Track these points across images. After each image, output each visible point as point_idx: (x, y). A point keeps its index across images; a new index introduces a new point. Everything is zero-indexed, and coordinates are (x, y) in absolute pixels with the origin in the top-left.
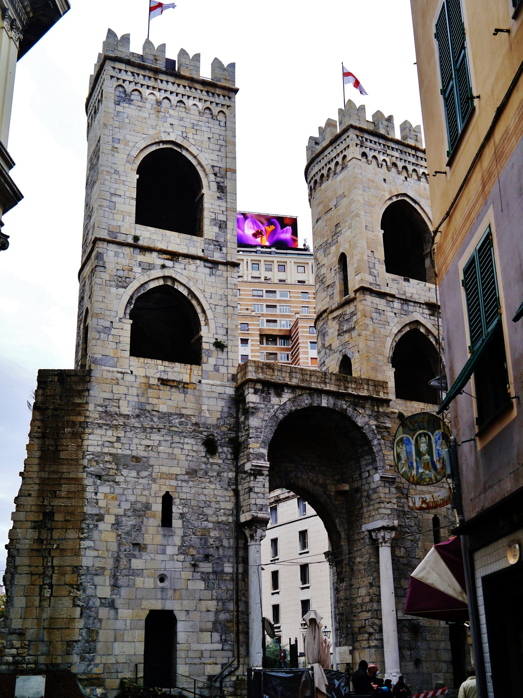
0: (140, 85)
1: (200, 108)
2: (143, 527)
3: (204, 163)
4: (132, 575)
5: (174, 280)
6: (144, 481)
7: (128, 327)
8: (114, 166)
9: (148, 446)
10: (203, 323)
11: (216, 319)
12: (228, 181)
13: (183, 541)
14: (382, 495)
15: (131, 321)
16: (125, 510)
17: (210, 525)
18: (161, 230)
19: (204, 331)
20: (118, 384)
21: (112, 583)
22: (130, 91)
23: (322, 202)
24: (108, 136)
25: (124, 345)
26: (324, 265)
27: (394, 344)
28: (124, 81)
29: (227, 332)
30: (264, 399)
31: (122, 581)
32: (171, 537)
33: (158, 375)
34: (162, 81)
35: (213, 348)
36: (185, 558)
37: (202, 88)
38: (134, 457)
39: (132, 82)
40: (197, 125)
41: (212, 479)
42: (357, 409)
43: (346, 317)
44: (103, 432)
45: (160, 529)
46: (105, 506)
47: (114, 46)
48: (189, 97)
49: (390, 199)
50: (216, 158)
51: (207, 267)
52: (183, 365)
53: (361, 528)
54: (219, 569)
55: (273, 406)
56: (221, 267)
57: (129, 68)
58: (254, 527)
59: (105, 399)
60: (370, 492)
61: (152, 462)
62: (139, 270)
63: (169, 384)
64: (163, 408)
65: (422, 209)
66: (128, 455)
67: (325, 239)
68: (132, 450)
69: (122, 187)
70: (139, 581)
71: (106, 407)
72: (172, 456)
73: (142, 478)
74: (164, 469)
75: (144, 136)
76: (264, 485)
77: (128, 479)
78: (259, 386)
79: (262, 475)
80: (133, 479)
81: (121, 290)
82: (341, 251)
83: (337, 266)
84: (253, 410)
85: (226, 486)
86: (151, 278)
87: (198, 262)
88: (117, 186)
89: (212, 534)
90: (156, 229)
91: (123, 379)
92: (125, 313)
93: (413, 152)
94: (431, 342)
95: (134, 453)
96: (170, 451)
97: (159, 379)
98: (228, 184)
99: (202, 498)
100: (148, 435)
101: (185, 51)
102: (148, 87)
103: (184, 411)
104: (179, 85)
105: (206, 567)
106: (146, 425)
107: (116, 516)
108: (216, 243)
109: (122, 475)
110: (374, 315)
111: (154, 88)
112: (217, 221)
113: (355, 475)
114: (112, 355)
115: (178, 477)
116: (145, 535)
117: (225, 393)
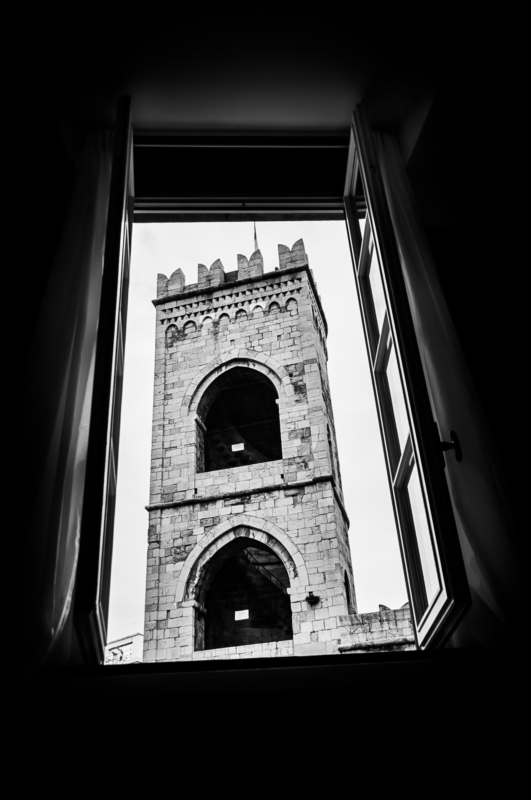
0: (193, 315)
1: (264, 307)
5: (249, 528)
8: (167, 416)
10: (291, 575)
11: (307, 563)
18: (226, 470)
22: (182, 326)
24: (159, 385)
25: (183, 638)
28: (176, 319)
29: (325, 578)
39: (184, 316)
40: (263, 328)
47: (163, 289)
48: (250, 302)
50: (290, 355)
51: (289, 496)
56: (307, 489)
57: (181, 303)
69: (178, 436)
75: (201, 368)
86: (216, 537)
87: (276, 493)
88: (172, 438)
90: (220, 471)
92: (187, 593)
101: (241, 255)
102: (202, 313)
104: (237, 295)
108: (298, 460)
111: (209, 311)
112: (298, 431)
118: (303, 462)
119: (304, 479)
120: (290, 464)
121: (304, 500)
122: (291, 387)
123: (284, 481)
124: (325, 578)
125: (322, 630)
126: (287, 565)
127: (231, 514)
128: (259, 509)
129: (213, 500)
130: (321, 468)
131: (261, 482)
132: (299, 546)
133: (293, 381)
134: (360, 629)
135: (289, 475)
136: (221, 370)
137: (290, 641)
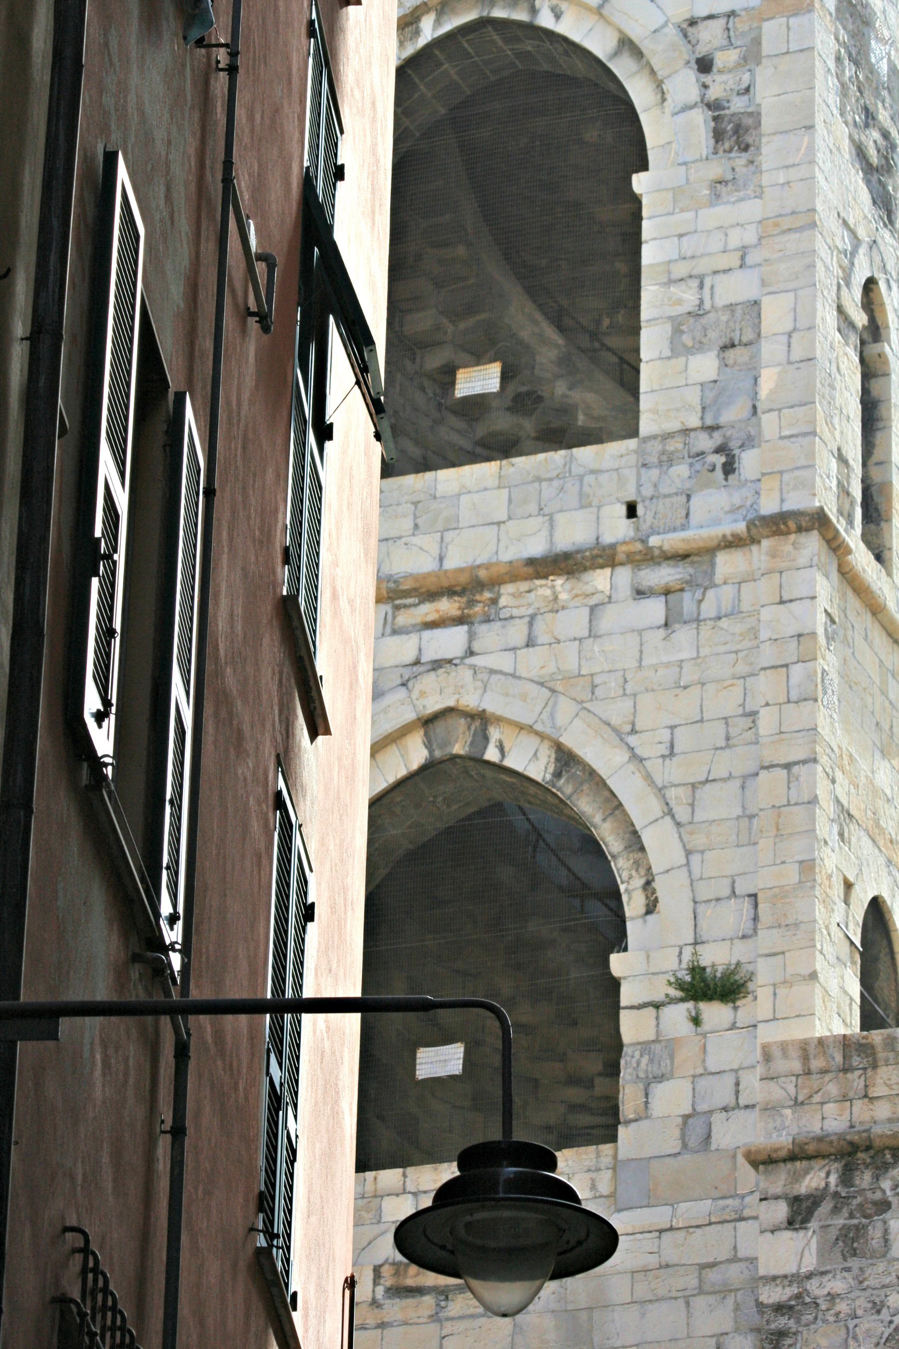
5: (481, 721)
11: (695, 859)
29: (756, 919)
30: (851, 1243)
84: (782, 1322)
87: (600, 580)
108: (705, 442)
118: (719, 450)
119: (717, 522)
120: (667, 460)
121: (708, 608)
122: (700, 119)
123: (637, 529)
124: (756, 919)
125: (725, 1109)
126: (623, 869)
127: (417, 662)
128: (530, 643)
130: (786, 477)
131: (545, 533)
132: (671, 793)
133: (714, 93)
134: (833, 1089)
135: (661, 506)
136: (417, 33)
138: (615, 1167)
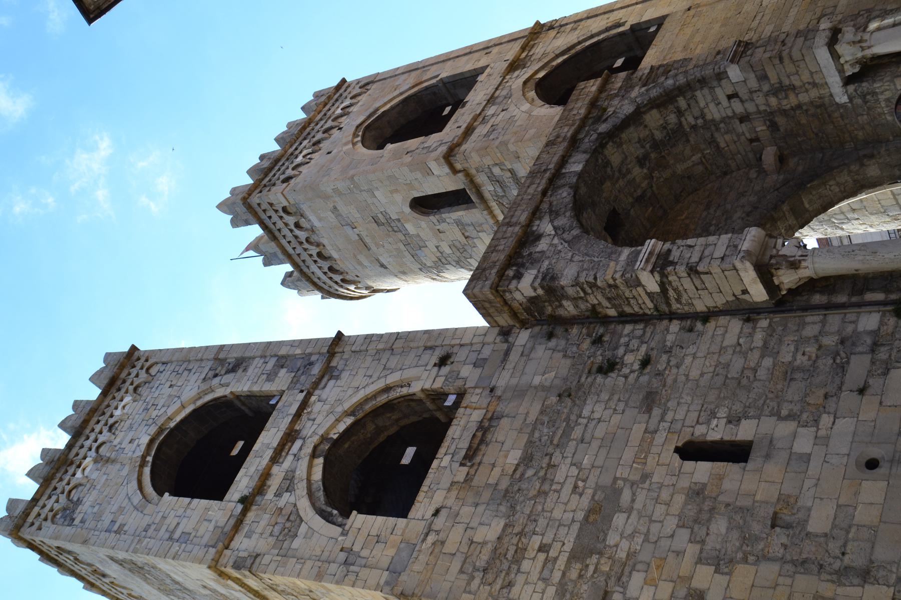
2: (738, 503)
3: (194, 392)
4: (848, 532)
5: (324, 438)
6: (641, 497)
7: (362, 517)
8: (137, 533)
9: (576, 487)
10: (405, 391)
12: (230, 356)
13: (790, 417)
14: (767, 55)
15: (354, 513)
16: (690, 541)
17: (768, 362)
19: (416, 388)
20: (443, 543)
21: (856, 581)
23: (355, 256)
26: (437, 247)
27: (547, 106)
28: (51, 510)
31: (855, 558)
32: (774, 443)
33: (456, 465)
34: (77, 454)
35: (445, 370)
36: (829, 413)
37: (111, 396)
38: (586, 518)
41: (671, 364)
42: (605, 117)
43: (499, 190)
44: (521, 579)
45: (750, 465)
46: (671, 585)
48: (112, 416)
49: (354, 144)
52: (455, 422)
53: (843, 106)
54: (869, 341)
55: (551, 245)
58: (773, 261)
59: (461, 571)
60: (766, 87)
61: (606, 480)
62: (286, 495)
63: (475, 446)
64: (514, 457)
65: (386, 104)
66: (580, 529)
67: (402, 247)
68: (573, 521)
69: (168, 521)
70: (862, 516)
71: (475, 569)
72: (608, 442)
73: (633, 501)
74: (628, 455)
76: (690, 246)
77: (629, 531)
78: (510, 273)
79: (669, 251)
80: (630, 521)
81: (303, 528)
82: (407, 210)
83: (432, 217)
85: (693, 335)
86: (305, 476)
87: (313, 398)
89: (788, 358)
91: (438, 532)
93: (312, 125)
94: (564, 62)
95: (580, 516)
96: (595, 444)
97: (462, 465)
98: (233, 356)
99: (707, 377)
100: (554, 487)
102: (74, 475)
103: (532, 418)
105: (859, 366)
106: (533, 493)
107: (699, 561)
108: (300, 372)
109: (617, 546)
110: (491, 137)
111: (79, 466)
113: (743, 133)
114: (391, 552)
115: (652, 427)
116: (758, 498)
117: (524, 346)
126: (393, 395)
127: (295, 455)
129: (266, 475)
137: (469, 391)
138: (475, 388)
